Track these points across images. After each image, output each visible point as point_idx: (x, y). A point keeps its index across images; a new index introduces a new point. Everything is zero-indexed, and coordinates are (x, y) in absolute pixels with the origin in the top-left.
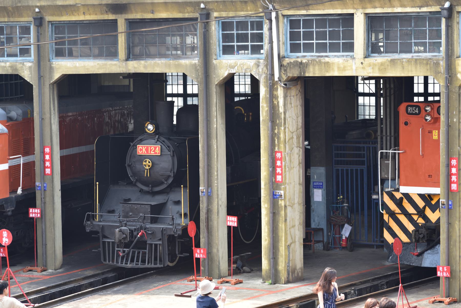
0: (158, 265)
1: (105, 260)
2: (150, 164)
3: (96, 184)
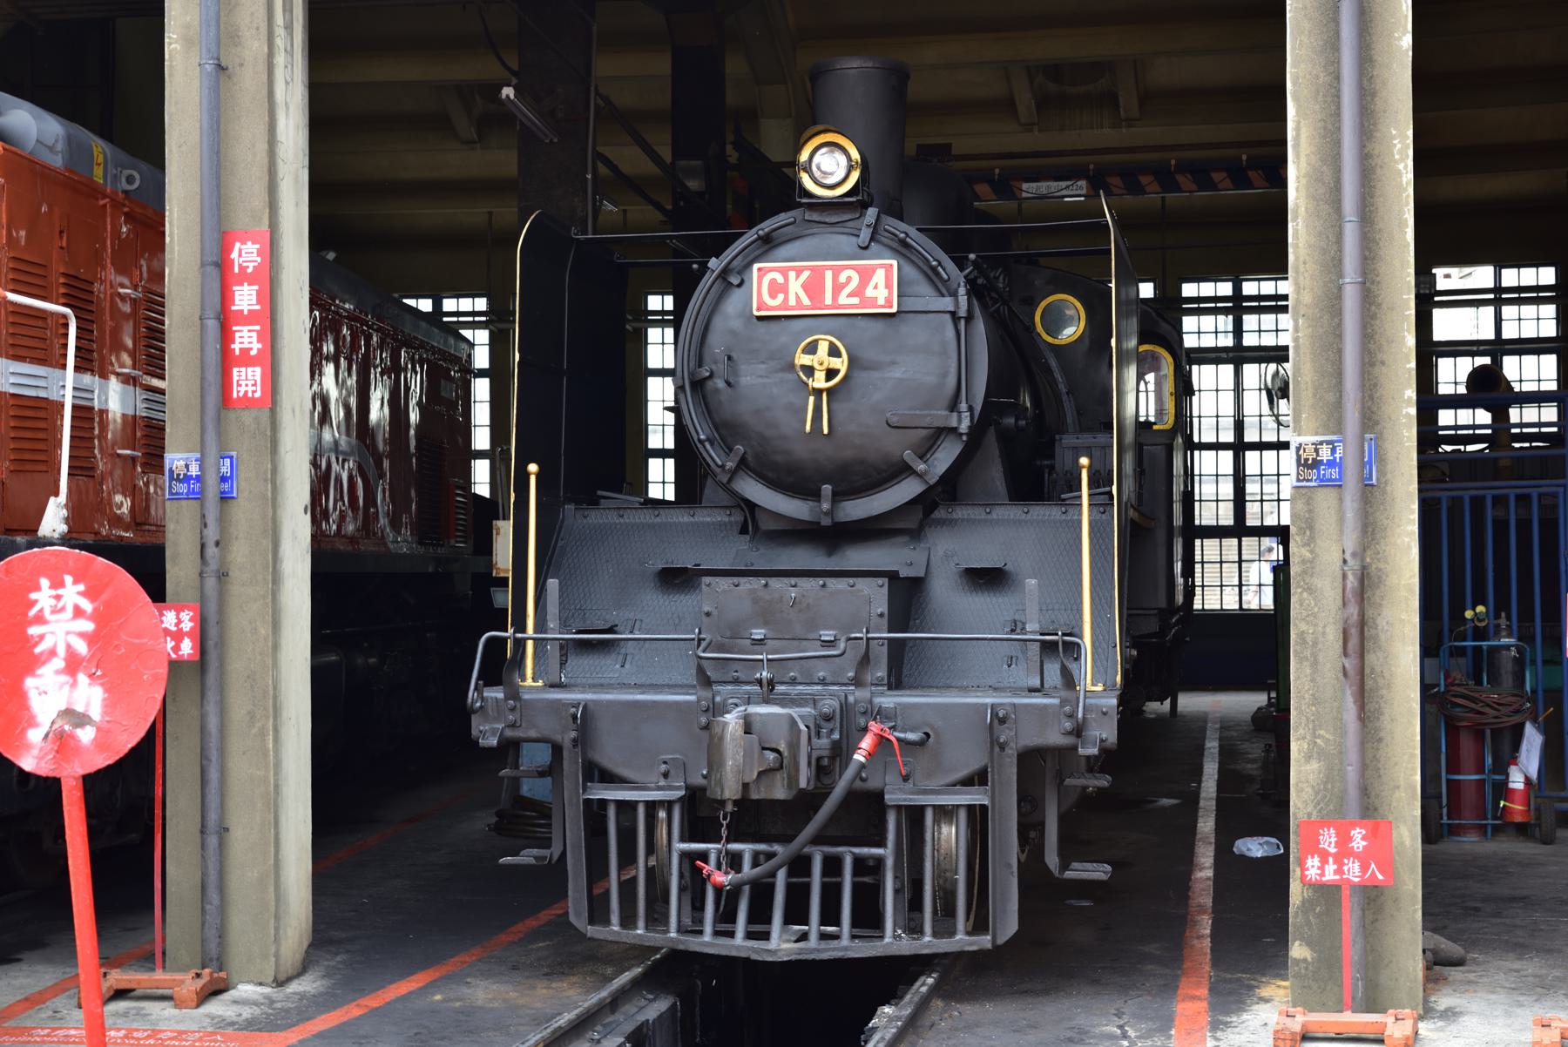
0: (962, 940)
1: (598, 912)
2: (841, 364)
3: (523, 477)
